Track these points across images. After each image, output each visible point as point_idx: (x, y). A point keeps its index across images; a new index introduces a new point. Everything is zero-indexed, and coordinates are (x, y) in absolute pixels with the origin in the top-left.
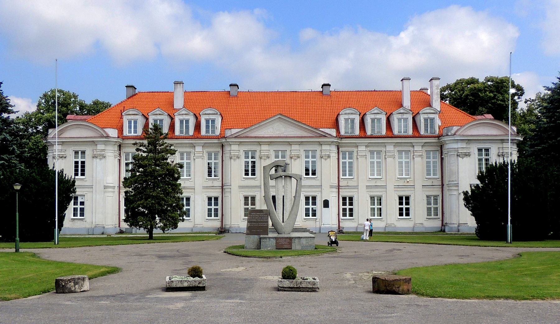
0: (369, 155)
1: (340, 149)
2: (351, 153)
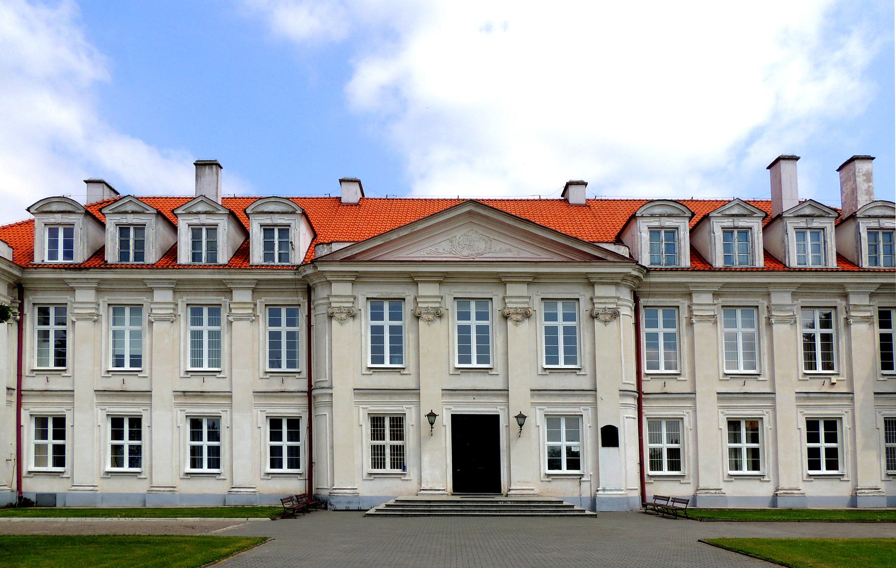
1: (642, 301)
2: (671, 311)
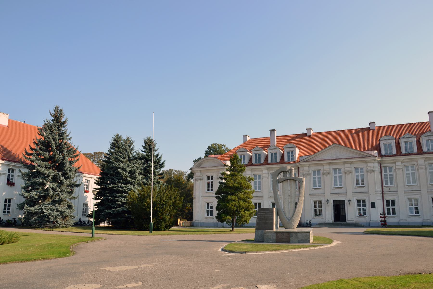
0: (405, 168)
1: (382, 165)
2: (390, 168)
